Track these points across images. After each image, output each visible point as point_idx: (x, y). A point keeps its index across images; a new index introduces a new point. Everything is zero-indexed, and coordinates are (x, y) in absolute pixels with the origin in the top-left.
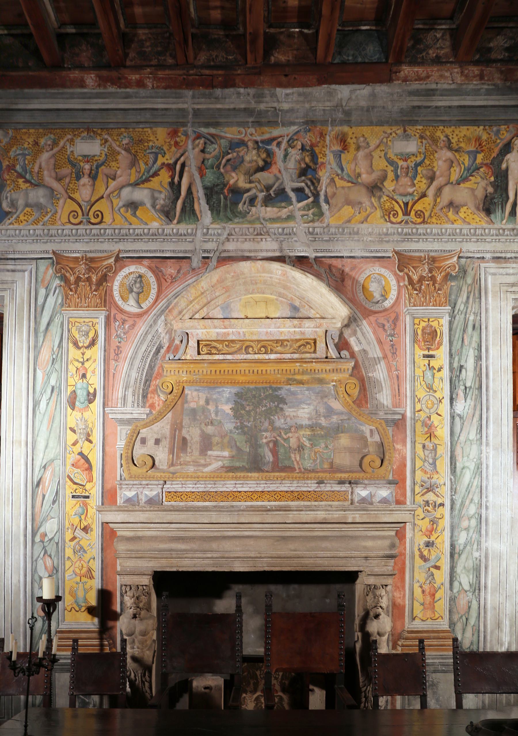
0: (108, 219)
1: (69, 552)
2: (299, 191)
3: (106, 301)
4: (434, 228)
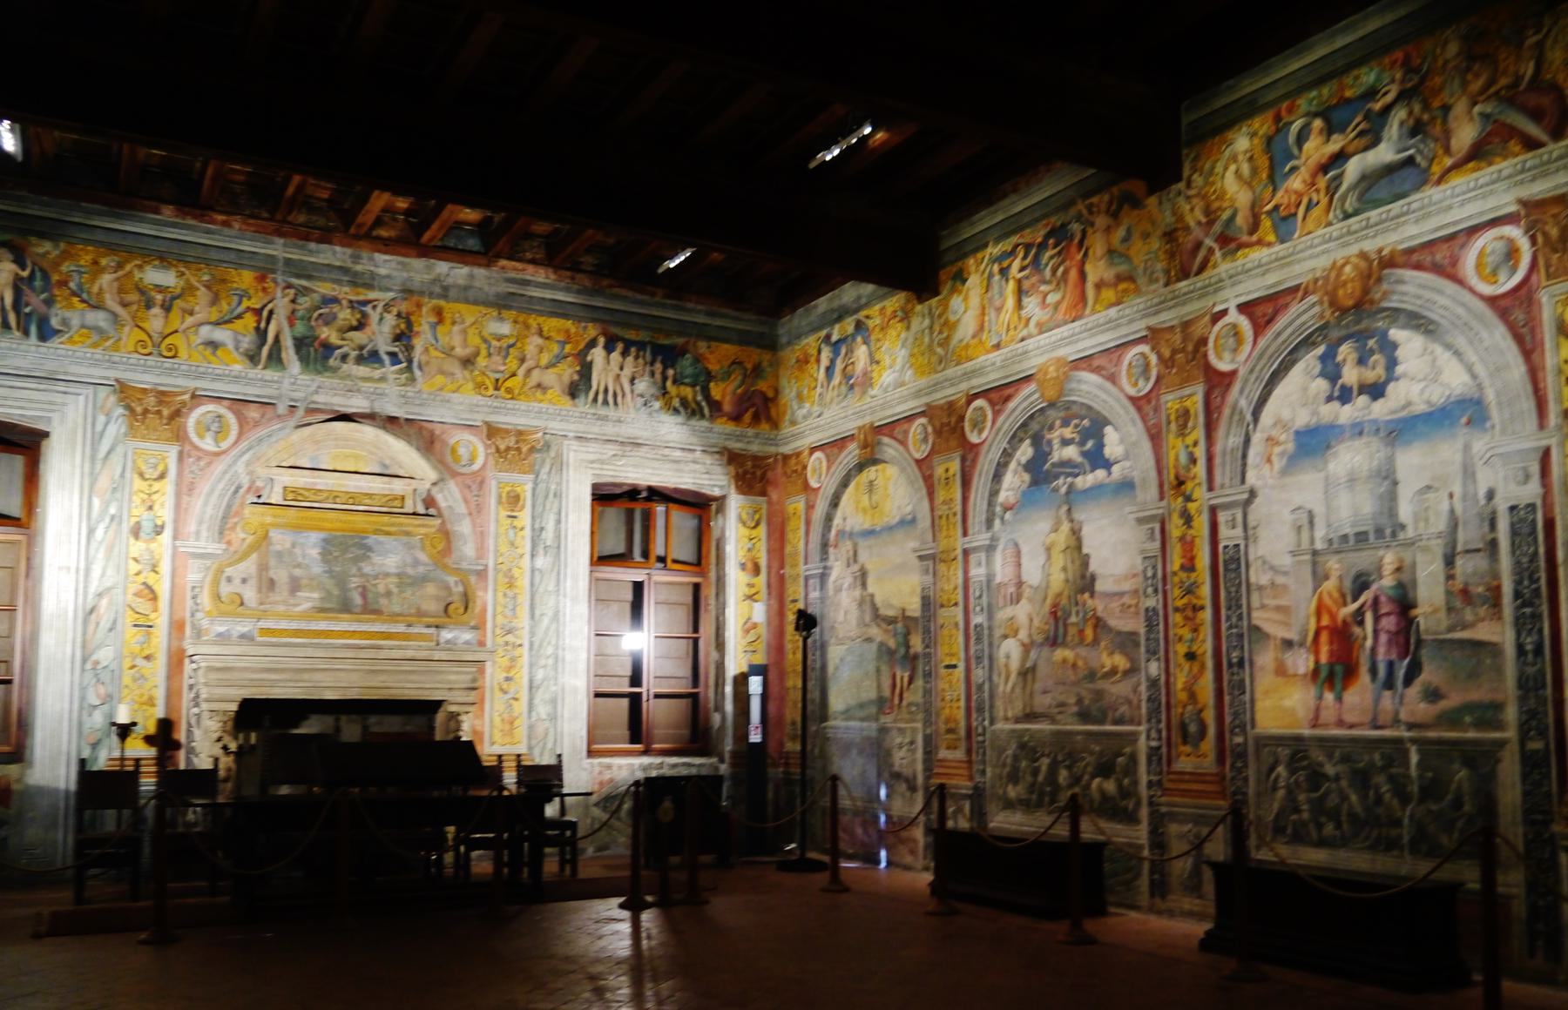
0: (183, 353)
1: (127, 680)
2: (392, 355)
3: (180, 437)
4: (521, 405)
